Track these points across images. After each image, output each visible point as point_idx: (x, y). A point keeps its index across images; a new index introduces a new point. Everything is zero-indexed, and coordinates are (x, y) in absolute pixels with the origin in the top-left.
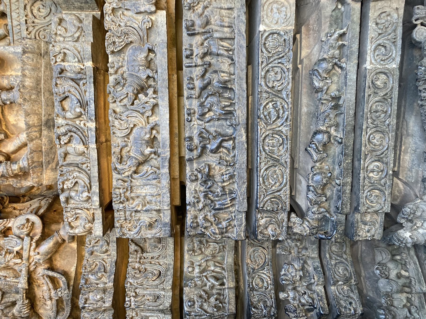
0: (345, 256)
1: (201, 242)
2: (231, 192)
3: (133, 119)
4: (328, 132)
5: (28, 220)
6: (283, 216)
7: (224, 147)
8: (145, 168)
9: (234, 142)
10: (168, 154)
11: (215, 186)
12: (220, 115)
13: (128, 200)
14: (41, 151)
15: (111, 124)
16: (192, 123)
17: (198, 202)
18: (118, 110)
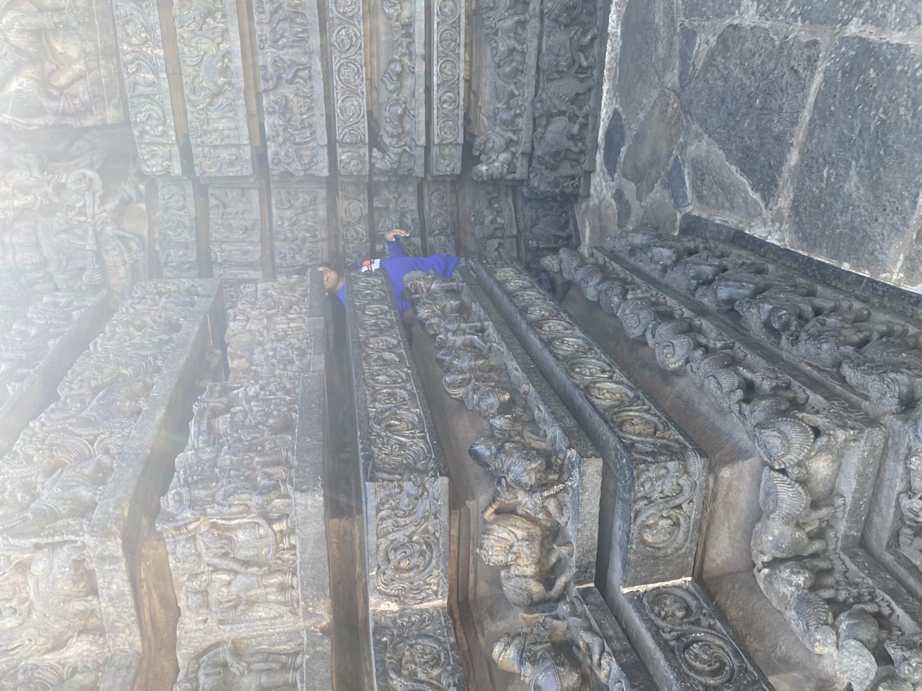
0: (445, 208)
1: (289, 193)
2: (310, 126)
3: (203, 46)
4: (400, 61)
5: (84, 175)
6: (365, 150)
7: (300, 77)
8: (221, 100)
9: (310, 71)
10: (242, 84)
11: (294, 119)
12: (293, 42)
13: (205, 134)
14: (101, 83)
15: (180, 51)
16: (265, 51)
17: (278, 135)
18: (185, 36)
